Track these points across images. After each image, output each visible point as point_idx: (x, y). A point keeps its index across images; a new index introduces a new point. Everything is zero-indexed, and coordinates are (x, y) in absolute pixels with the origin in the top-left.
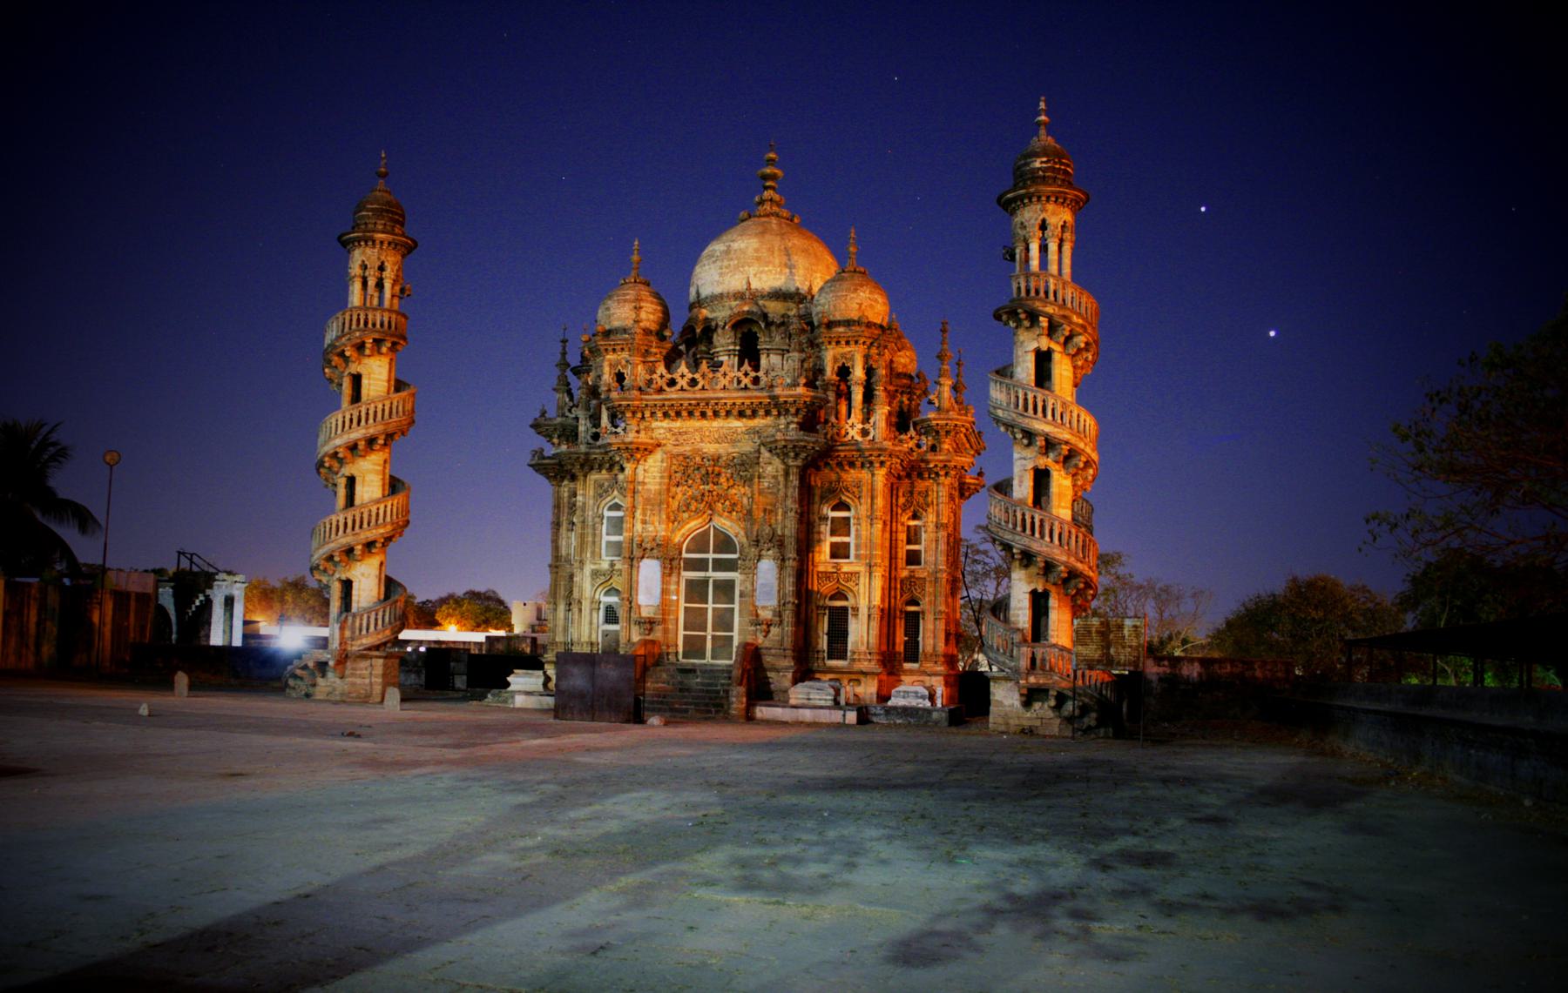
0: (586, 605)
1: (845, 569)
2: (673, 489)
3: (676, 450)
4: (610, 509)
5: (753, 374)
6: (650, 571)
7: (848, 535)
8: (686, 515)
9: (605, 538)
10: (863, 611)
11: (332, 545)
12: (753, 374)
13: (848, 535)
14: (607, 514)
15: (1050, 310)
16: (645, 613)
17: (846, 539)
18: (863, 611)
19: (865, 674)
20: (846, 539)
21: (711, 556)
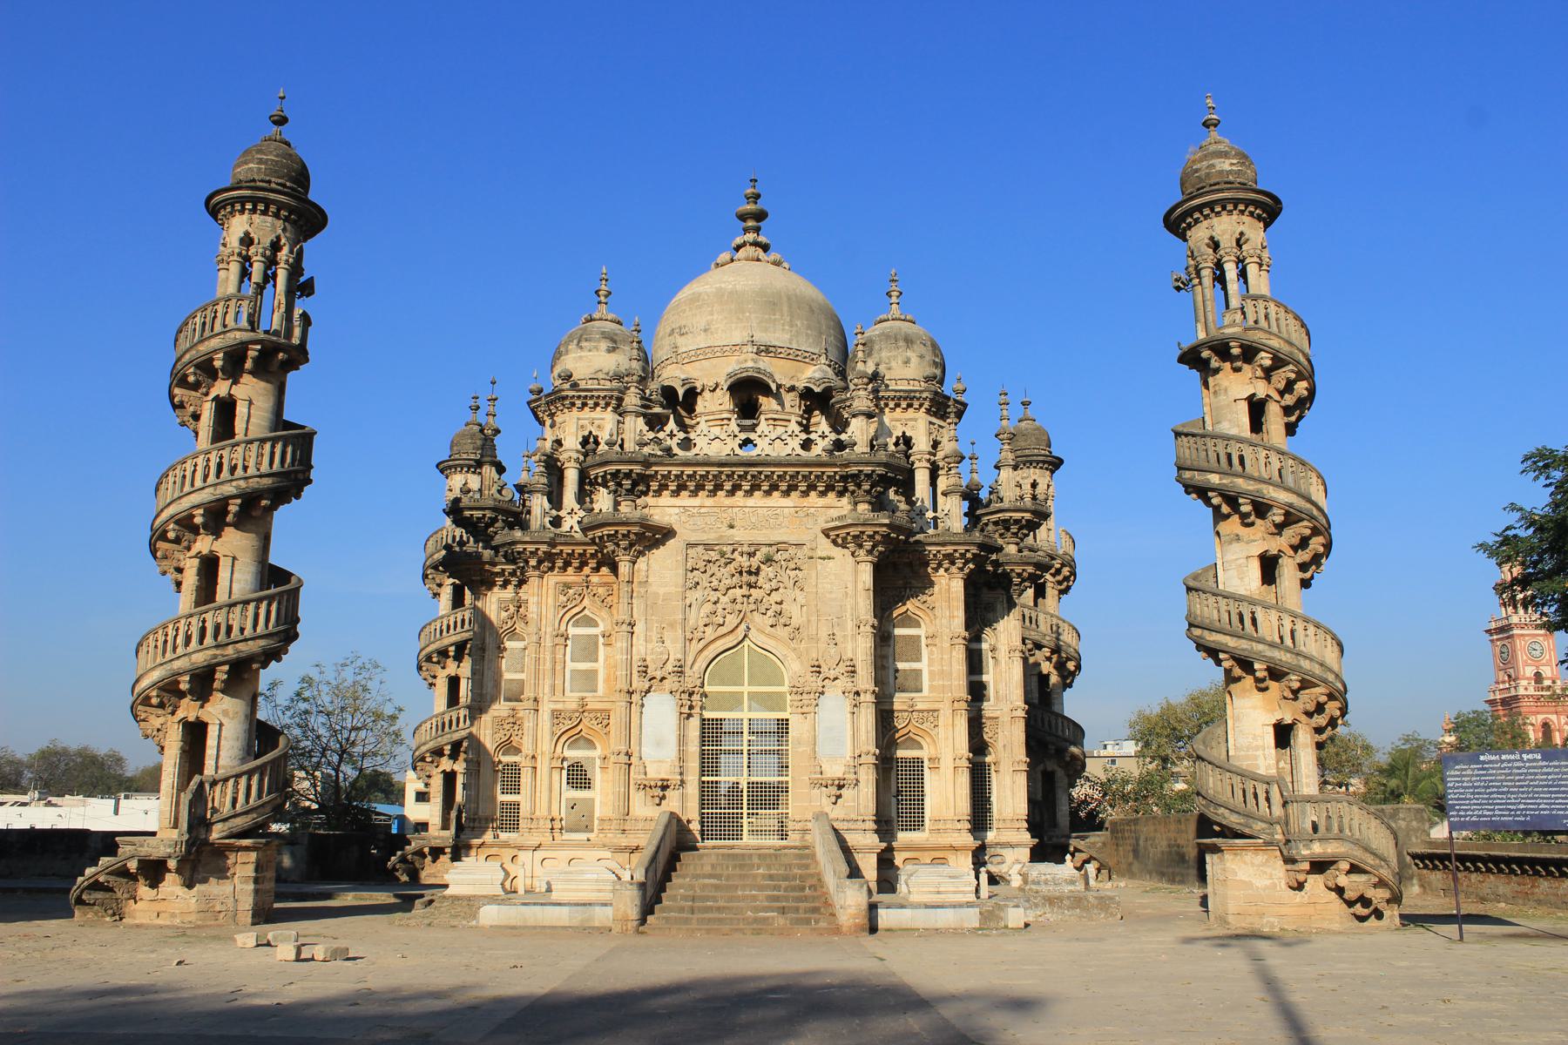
0: (543, 765)
1: (920, 706)
2: (693, 596)
3: (693, 539)
4: (576, 624)
5: (804, 436)
6: (661, 712)
7: (919, 660)
8: (709, 630)
9: (570, 665)
10: (947, 764)
11: (177, 665)
12: (804, 436)
13: (919, 660)
14: (572, 631)
15: (1275, 343)
16: (655, 773)
17: (915, 665)
18: (947, 764)
19: (953, 848)
20: (915, 665)
21: (746, 689)
